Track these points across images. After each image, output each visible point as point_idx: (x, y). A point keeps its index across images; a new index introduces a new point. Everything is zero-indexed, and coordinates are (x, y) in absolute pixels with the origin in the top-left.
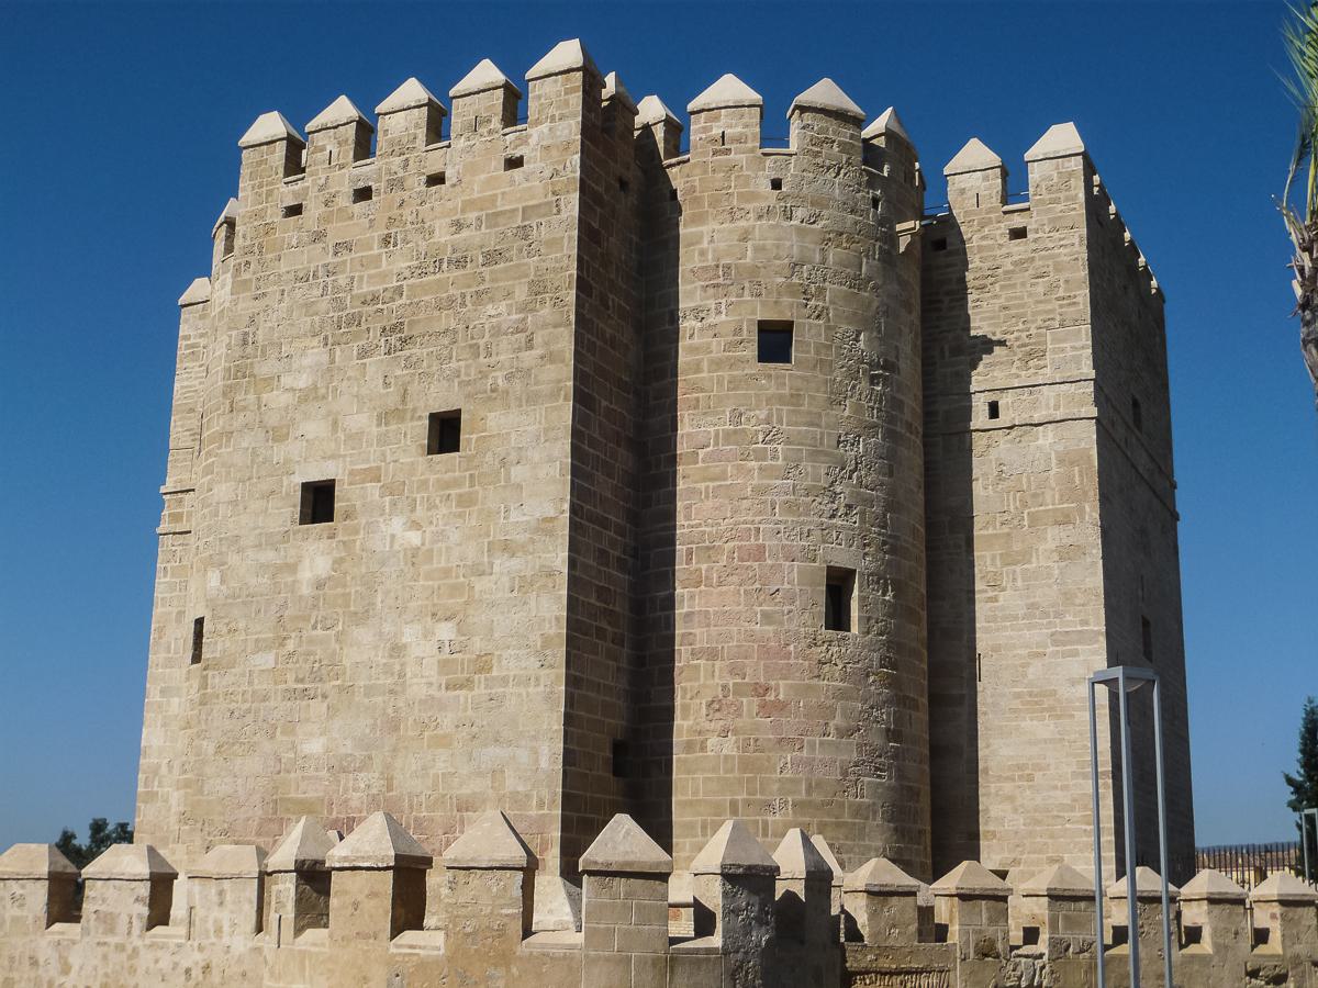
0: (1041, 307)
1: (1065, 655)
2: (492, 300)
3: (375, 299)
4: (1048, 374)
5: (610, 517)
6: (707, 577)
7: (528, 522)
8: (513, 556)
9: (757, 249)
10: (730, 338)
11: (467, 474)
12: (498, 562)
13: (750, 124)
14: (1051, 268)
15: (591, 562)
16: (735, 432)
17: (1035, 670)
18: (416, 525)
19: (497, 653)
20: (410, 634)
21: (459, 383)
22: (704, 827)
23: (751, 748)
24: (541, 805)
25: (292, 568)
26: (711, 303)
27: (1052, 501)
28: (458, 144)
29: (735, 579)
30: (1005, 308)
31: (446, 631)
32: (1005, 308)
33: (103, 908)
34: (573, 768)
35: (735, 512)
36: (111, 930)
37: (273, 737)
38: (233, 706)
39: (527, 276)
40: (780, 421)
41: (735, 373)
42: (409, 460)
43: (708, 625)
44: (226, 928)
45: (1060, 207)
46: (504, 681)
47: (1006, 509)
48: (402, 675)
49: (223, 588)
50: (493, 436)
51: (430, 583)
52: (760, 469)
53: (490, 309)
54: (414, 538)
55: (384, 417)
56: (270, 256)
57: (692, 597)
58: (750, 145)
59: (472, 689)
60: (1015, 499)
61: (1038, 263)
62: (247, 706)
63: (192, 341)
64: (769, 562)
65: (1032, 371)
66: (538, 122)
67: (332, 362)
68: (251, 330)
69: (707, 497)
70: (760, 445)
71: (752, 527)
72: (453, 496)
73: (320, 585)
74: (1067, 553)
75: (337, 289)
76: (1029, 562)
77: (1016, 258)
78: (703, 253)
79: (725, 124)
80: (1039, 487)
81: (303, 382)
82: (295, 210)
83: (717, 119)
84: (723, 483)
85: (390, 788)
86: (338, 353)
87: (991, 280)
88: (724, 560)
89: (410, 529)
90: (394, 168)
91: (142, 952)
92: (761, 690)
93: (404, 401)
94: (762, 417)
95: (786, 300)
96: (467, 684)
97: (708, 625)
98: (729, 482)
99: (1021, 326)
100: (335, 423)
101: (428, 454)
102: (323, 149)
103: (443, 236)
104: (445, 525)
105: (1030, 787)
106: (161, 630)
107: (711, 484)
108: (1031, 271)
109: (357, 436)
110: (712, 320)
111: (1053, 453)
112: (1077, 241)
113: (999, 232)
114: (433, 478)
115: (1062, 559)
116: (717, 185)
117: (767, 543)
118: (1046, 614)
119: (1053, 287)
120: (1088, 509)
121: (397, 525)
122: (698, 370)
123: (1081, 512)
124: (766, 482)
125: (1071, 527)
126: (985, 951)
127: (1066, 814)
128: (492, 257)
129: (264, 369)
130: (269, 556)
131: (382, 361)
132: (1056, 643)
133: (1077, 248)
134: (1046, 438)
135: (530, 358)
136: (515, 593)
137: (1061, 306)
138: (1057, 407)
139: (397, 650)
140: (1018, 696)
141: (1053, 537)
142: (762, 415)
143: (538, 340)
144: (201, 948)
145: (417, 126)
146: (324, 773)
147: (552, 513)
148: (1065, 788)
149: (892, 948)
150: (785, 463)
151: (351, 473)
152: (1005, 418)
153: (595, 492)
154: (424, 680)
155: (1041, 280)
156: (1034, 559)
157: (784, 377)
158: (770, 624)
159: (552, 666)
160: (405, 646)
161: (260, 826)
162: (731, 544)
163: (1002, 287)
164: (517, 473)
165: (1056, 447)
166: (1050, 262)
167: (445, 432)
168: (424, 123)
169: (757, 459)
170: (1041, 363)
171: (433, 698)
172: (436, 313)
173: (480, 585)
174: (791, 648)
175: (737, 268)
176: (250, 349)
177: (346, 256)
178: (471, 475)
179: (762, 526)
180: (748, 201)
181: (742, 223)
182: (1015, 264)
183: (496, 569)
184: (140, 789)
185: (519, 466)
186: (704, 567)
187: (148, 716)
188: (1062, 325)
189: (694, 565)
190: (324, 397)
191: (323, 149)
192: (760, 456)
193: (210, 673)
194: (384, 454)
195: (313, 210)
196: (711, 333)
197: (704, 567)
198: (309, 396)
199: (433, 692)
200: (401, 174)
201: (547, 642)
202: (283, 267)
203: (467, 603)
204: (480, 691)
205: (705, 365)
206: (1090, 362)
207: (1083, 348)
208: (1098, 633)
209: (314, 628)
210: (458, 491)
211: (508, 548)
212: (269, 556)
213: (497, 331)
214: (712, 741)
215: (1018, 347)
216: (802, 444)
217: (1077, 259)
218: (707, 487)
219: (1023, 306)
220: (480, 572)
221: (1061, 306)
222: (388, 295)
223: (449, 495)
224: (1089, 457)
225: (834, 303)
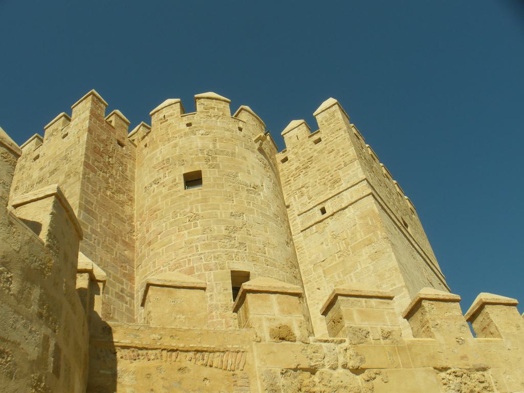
4: (344, 186)
9: (180, 148)
16: (175, 221)
27: (361, 236)
30: (319, 170)
32: (319, 170)
40: (197, 210)
41: (173, 197)
45: (332, 125)
47: (339, 250)
52: (189, 233)
58: (176, 115)
60: (342, 244)
61: (328, 148)
64: (196, 273)
65: (337, 188)
71: (186, 260)
76: (357, 268)
78: (157, 159)
80: (353, 234)
84: (171, 244)
94: (188, 211)
98: (173, 243)
107: (165, 248)
111: (356, 216)
112: (343, 132)
115: (373, 260)
117: (195, 265)
120: (379, 233)
124: (192, 237)
125: (373, 244)
126: (284, 335)
138: (352, 197)
141: (366, 252)
142: (188, 210)
149: (179, 330)
150: (201, 228)
152: (329, 212)
156: (359, 267)
157: (198, 193)
163: (315, 164)
165: (357, 213)
166: (334, 145)
169: (186, 229)
170: (340, 183)
174: (214, 313)
175: (172, 158)
179: (191, 258)
180: (176, 134)
188: (345, 165)
206: (362, 173)
207: (357, 169)
208: (402, 287)
215: (328, 182)
216: (210, 218)
224: (373, 211)
225: (222, 162)
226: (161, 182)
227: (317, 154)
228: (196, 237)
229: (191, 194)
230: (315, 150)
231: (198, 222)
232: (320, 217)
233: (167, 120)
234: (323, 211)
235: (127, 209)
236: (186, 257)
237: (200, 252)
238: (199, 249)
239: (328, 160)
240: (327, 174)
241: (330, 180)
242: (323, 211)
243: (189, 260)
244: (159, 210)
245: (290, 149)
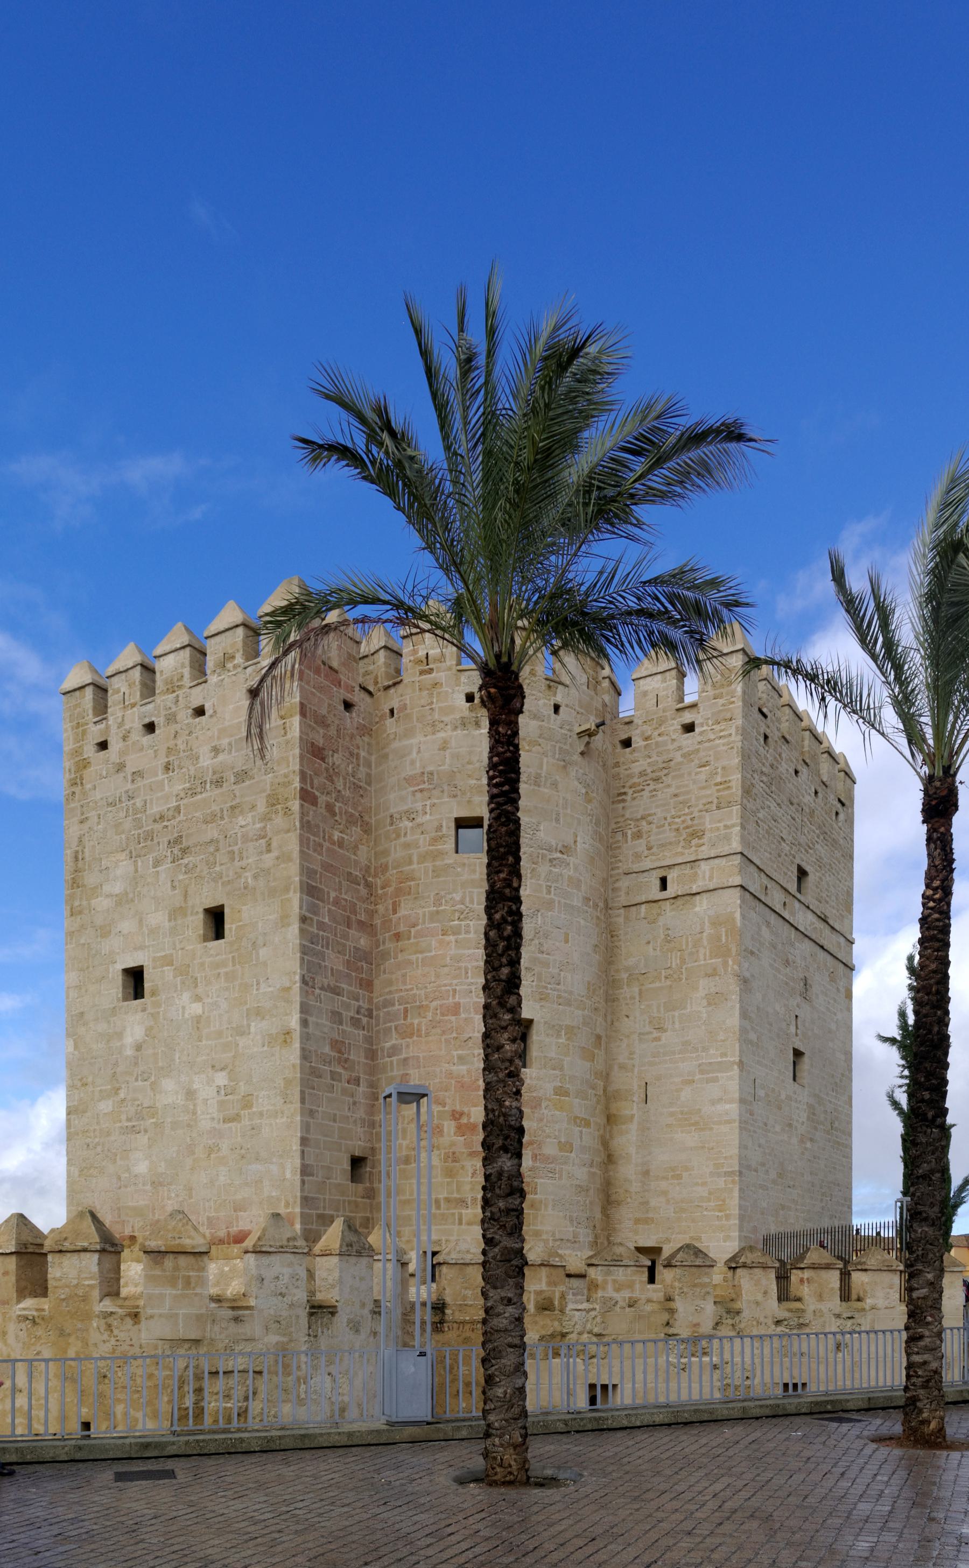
0: (704, 792)
5: (343, 985)
6: (418, 1030)
7: (272, 992)
8: (263, 1018)
10: (434, 834)
11: (230, 956)
12: (253, 1024)
14: (712, 758)
15: (324, 1021)
16: (438, 912)
19: (255, 1094)
21: (223, 884)
23: (450, 1160)
29: (439, 1031)
34: (311, 1178)
35: (438, 976)
40: (472, 902)
42: (191, 947)
43: (419, 1067)
50: (245, 925)
51: (210, 1042)
57: (408, 1046)
59: (240, 1122)
61: (702, 754)
64: (463, 1016)
69: (417, 966)
70: (456, 922)
72: (222, 975)
77: (685, 751)
87: (666, 771)
89: (195, 1001)
94: (458, 899)
97: (419, 1067)
98: (433, 953)
99: (687, 810)
101: (204, 941)
104: (218, 997)
105: (678, 1184)
107: (420, 956)
108: (697, 762)
113: (672, 728)
114: (208, 960)
117: (462, 1001)
119: (714, 774)
122: (411, 863)
127: (704, 1204)
131: (169, 868)
133: (733, 738)
136: (265, 1048)
137: (718, 791)
142: (457, 897)
153: (325, 966)
154: (208, 1116)
155: (703, 769)
157: (475, 865)
158: (463, 1064)
159: (291, 1102)
162: (434, 1004)
166: (711, 753)
170: (701, 842)
173: (242, 1041)
178: (233, 957)
182: (683, 756)
183: (253, 1029)
185: (265, 948)
186: (416, 1022)
192: (456, 931)
196: (420, 831)
201: (288, 1082)
203: (234, 1057)
204: (246, 1122)
205: (415, 859)
210: (225, 970)
211: (259, 1013)
215: (684, 828)
217: (732, 748)
218: (417, 959)
219: (688, 793)
220: (241, 1031)
221: (718, 791)
223: (219, 974)
227: (679, 759)
228: (467, 952)
229: (464, 864)
230: (680, 748)
231: (471, 923)
235: (363, 855)
236: (451, 985)
237: (470, 980)
238: (470, 975)
239: (694, 782)
240: (687, 810)
241: (687, 827)
243: (455, 991)
244: (413, 879)
245: (640, 722)
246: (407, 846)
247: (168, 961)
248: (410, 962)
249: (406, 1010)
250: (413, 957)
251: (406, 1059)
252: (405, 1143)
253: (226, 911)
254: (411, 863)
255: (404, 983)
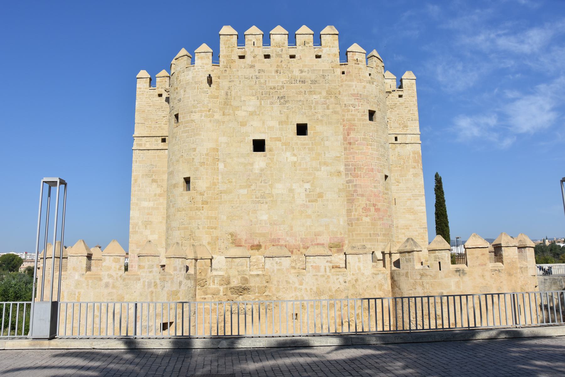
1: (416, 199)
2: (315, 94)
3: (274, 88)
4: (408, 132)
13: (362, 58)
17: (408, 203)
18: (295, 155)
20: (295, 186)
22: (363, 240)
24: (341, 234)
25: (252, 164)
26: (357, 103)
28: (299, 47)
31: (307, 186)
33: (314, 264)
35: (366, 158)
36: (319, 271)
37: (248, 214)
38: (232, 205)
39: (325, 89)
44: (362, 268)
46: (328, 200)
48: (293, 197)
49: (226, 169)
53: (315, 96)
54: (295, 159)
55: (281, 123)
56: (234, 70)
62: (238, 205)
63: (142, 90)
66: (325, 47)
67: (261, 104)
68: (229, 91)
73: (262, 170)
74: (415, 175)
75: (260, 83)
78: (354, 90)
79: (357, 56)
81: (251, 109)
82: (242, 57)
83: (355, 55)
85: (292, 230)
86: (263, 102)
88: (364, 171)
90: (278, 51)
91: (331, 277)
92: (374, 205)
93: (287, 119)
95: (374, 106)
96: (316, 201)
100: (263, 123)
102: (251, 40)
103: (297, 73)
106: (136, 180)
109: (275, 128)
110: (357, 108)
116: (357, 72)
118: (411, 190)
121: (288, 154)
123: (418, 165)
128: (314, 82)
129: (235, 103)
130: (242, 160)
132: (413, 197)
134: (409, 147)
135: (328, 112)
139: (291, 190)
140: (404, 209)
141: (412, 171)
143: (331, 107)
144: (353, 274)
145: (284, 40)
146: (268, 225)
147: (339, 155)
148: (417, 231)
151: (271, 138)
152: (399, 141)
160: (294, 189)
161: (246, 240)
162: (366, 167)
164: (327, 143)
167: (302, 130)
168: (287, 39)
171: (304, 204)
172: (296, 95)
176: (229, 97)
177: (262, 74)
181: (363, 84)
184: (131, 230)
186: (359, 173)
187: (132, 207)
189: (356, 172)
190: (258, 115)
191: (251, 40)
192: (371, 145)
193: (223, 195)
194: (282, 134)
195: (249, 59)
197: (359, 173)
198: (252, 114)
199: (304, 202)
200: (280, 53)
202: (240, 74)
205: (356, 119)
209: (261, 182)
211: (326, 164)
212: (242, 160)
213: (317, 103)
214: (364, 218)
222: (279, 87)
226: (357, 108)
232: (394, 141)
233: (359, 64)
234: (396, 139)
242: (396, 139)
246: (353, 115)
247: (279, 139)
248: (356, 153)
249: (355, 168)
250: (357, 151)
251: (355, 185)
252: (356, 213)
253: (308, 126)
254: (354, 120)
255: (354, 159)
